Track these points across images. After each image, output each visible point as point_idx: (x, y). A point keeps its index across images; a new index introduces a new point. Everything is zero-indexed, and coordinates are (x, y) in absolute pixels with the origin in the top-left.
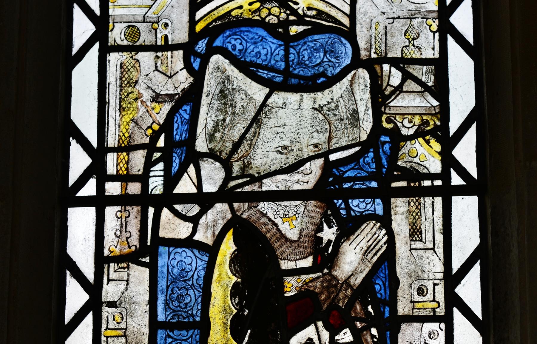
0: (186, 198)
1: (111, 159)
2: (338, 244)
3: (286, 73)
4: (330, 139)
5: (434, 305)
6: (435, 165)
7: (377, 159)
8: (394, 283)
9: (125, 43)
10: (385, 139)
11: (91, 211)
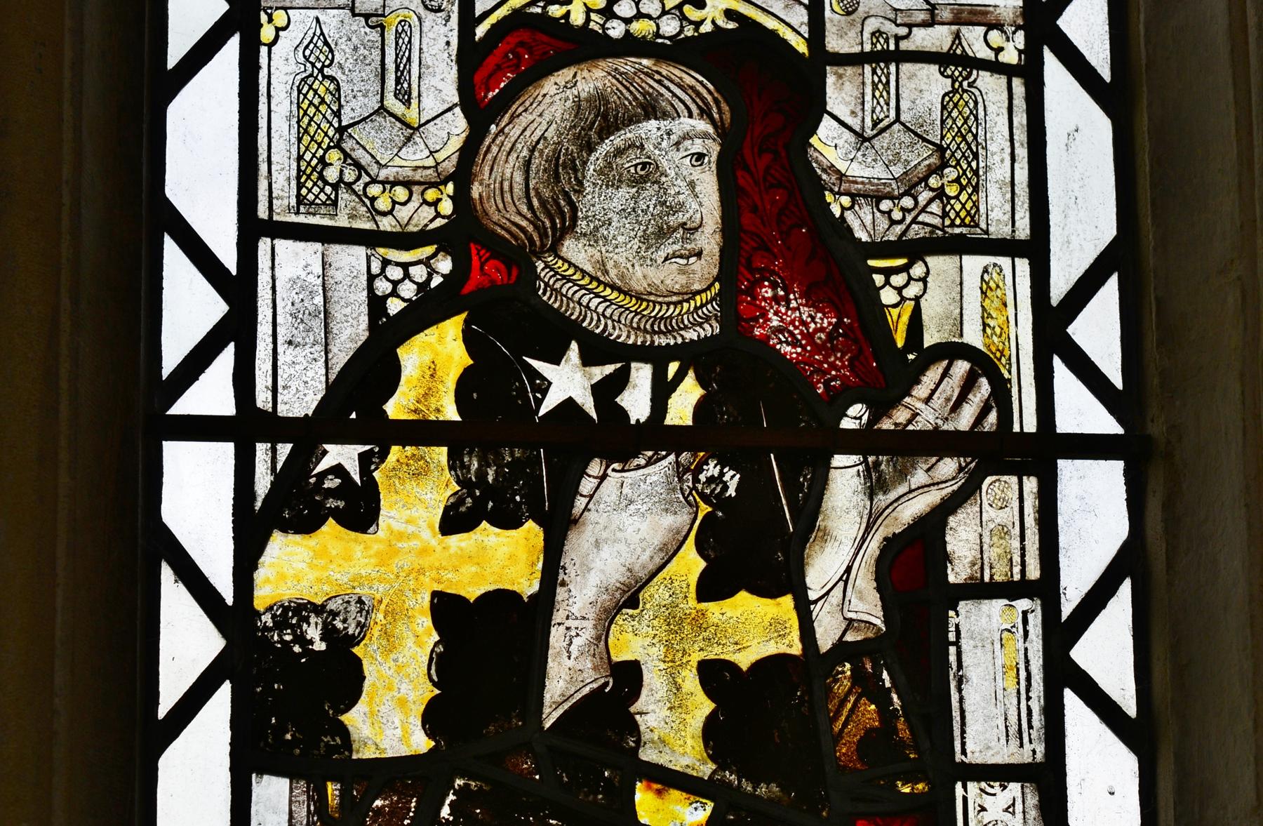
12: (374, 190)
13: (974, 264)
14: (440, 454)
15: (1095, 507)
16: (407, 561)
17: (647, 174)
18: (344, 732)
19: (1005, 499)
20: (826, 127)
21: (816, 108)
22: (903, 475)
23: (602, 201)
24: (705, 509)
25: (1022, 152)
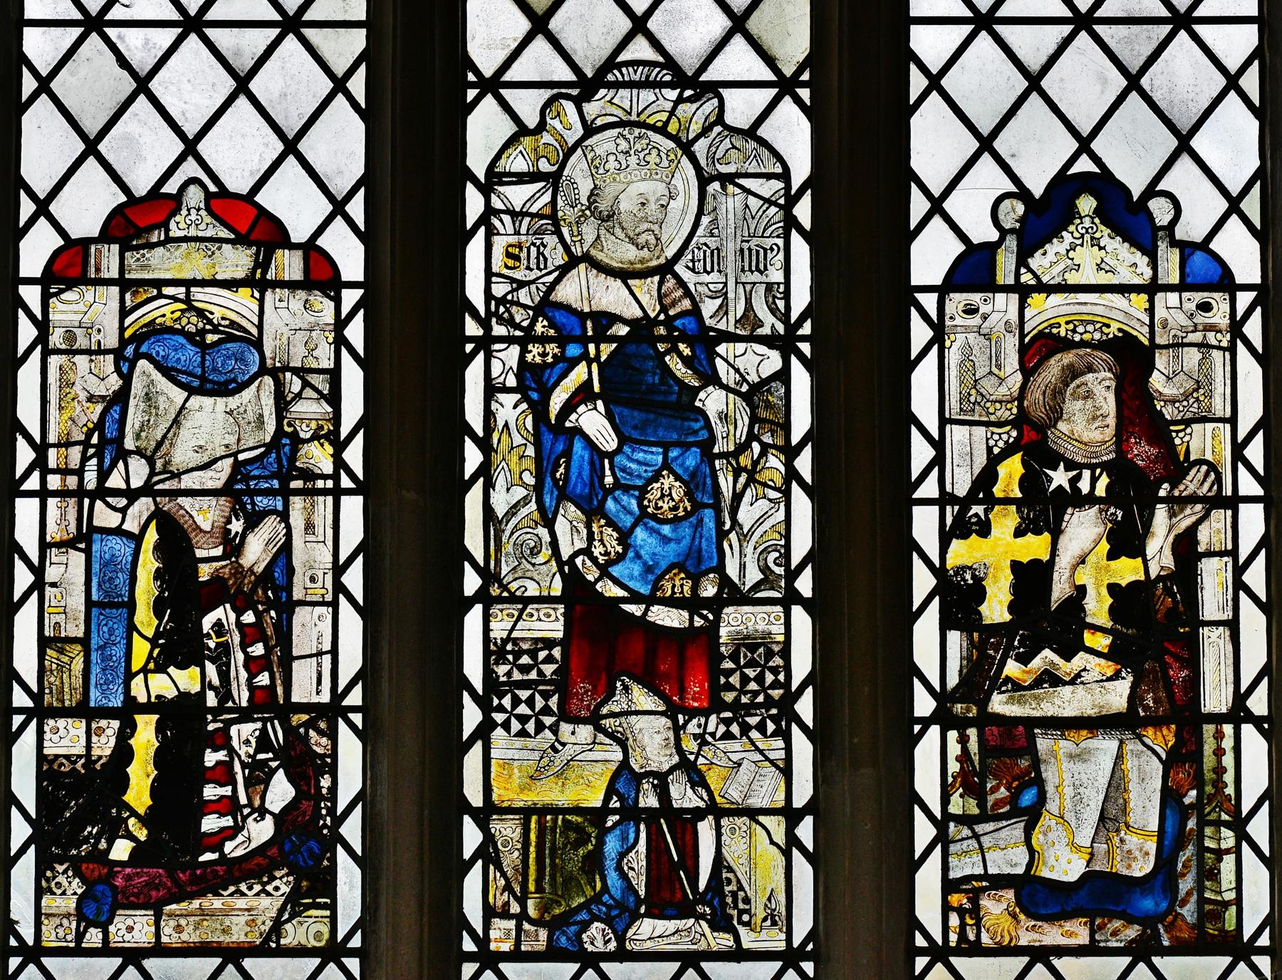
0: (116, 493)
1: (52, 453)
2: (244, 536)
3: (203, 378)
4: (239, 440)
5: (324, 591)
6: (328, 468)
7: (279, 459)
8: (291, 571)
9: (64, 347)
10: (285, 443)
11: (36, 502)
12: (988, 405)
13: (1209, 426)
14: (1014, 508)
15: (1253, 521)
16: (1002, 549)
17: (1089, 395)
18: (979, 613)
19: (1220, 517)
20: (1155, 374)
21: (1151, 367)
22: (1182, 510)
23: (1073, 406)
24: (1110, 525)
25: (1228, 382)
